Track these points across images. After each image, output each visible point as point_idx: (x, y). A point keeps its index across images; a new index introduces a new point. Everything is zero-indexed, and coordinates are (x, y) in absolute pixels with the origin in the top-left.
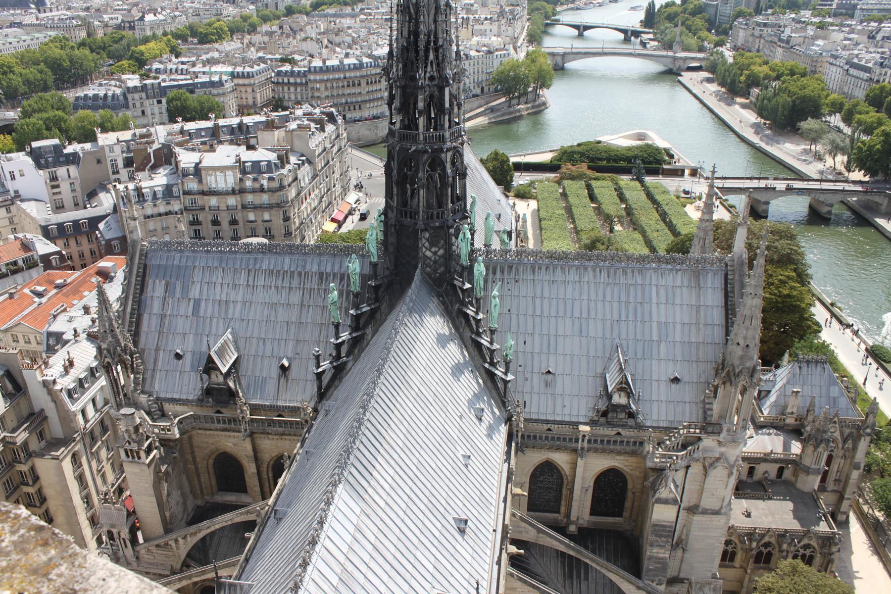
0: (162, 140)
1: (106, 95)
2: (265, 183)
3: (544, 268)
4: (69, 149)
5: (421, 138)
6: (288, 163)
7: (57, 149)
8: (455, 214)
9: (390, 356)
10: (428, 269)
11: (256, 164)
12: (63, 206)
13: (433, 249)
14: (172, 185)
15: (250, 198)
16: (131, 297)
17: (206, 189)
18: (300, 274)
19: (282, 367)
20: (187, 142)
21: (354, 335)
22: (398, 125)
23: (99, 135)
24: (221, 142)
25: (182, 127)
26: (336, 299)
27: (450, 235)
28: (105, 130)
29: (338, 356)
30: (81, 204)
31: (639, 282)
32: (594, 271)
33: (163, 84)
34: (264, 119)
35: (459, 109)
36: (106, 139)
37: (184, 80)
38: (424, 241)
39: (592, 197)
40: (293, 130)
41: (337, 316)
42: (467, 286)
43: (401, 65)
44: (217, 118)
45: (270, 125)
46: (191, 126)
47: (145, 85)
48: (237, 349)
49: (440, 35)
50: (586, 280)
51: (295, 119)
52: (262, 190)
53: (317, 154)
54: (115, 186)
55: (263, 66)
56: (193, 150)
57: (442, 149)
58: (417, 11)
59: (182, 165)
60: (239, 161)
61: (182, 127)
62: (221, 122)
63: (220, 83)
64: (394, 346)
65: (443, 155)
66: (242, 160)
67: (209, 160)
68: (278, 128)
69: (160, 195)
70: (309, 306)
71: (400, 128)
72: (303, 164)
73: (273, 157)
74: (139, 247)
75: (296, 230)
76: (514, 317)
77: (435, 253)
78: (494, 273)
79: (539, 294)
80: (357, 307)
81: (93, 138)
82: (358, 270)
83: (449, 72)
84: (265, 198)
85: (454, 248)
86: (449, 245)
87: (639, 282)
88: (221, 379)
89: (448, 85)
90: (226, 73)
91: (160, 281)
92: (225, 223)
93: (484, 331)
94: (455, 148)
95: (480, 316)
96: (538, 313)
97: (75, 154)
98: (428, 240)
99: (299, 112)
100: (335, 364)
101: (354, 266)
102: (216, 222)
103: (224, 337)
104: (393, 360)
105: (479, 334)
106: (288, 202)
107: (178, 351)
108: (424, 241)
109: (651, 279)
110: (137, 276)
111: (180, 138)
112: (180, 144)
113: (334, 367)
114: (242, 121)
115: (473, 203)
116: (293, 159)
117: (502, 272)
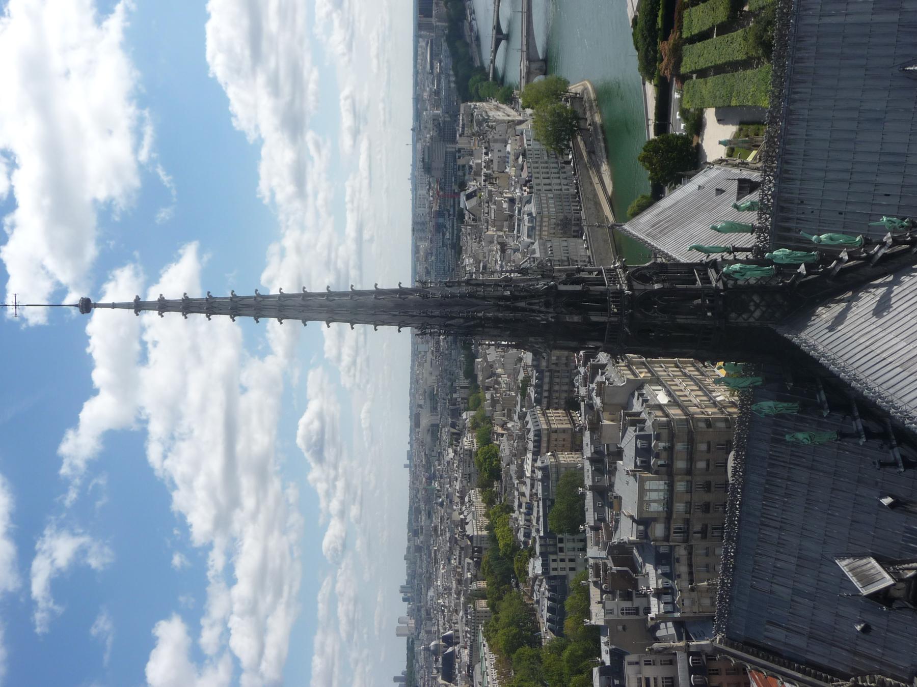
0: (603, 554)
1: (549, 599)
2: (661, 445)
3: (786, 167)
4: (606, 658)
5: (616, 319)
6: (639, 414)
7: (604, 671)
8: (708, 278)
9: (886, 394)
10: (777, 315)
11: (638, 452)
12: (672, 678)
13: (752, 308)
14: (657, 553)
15: (680, 464)
16: (784, 669)
17: (665, 515)
18: (772, 465)
19: (891, 505)
20: (607, 526)
21: (857, 414)
22: (599, 344)
23: (593, 622)
24: (612, 485)
25: (591, 527)
26: (806, 436)
27: (736, 286)
28: (588, 614)
29: (884, 436)
30: (671, 657)
31: (814, 40)
32: (794, 101)
33: (542, 534)
34: (587, 434)
35: (583, 271)
36: (598, 617)
37: (538, 510)
38: (740, 320)
39: (704, 36)
40: (602, 402)
41: (828, 436)
42: (802, 269)
43: (531, 339)
44: (583, 486)
45: (595, 427)
46: (590, 517)
47: (541, 554)
48: (862, 556)
49: (499, 293)
50: (806, 112)
51: (591, 398)
52: (670, 450)
53: (631, 377)
54: (652, 619)
55: (528, 418)
56: (617, 521)
57: (628, 294)
58: (474, 318)
59: (633, 538)
60: (633, 473)
61: (592, 528)
62: (588, 482)
63: (544, 469)
64: (873, 385)
65: (637, 293)
66: (632, 468)
67: (630, 507)
68: (599, 420)
69: (667, 569)
70: (814, 460)
71: (602, 340)
72: (641, 395)
73: (631, 432)
74: (722, 646)
75: (722, 413)
76: (850, 208)
77: (757, 306)
78: (789, 230)
79: (820, 174)
80: (820, 406)
81: (596, 631)
82: (771, 403)
83: (541, 285)
84: (679, 447)
85: (752, 281)
86: (749, 289)
87: (814, 40)
88: (902, 585)
89: (555, 286)
90: (534, 460)
91: (766, 630)
92: (708, 497)
93: (865, 251)
94: (629, 279)
95: (844, 255)
96: (847, 176)
97: (612, 653)
98: (740, 315)
99: (583, 391)
100: (894, 443)
101: (767, 406)
102: (706, 508)
103: (845, 570)
104: (892, 391)
105: (870, 258)
106: (687, 420)
107: (858, 628)
108: (740, 320)
109: (812, 25)
110: (757, 656)
111: (603, 534)
112: (610, 536)
113: (899, 444)
114: (588, 458)
115: (699, 249)
116: (637, 406)
117: (788, 219)
